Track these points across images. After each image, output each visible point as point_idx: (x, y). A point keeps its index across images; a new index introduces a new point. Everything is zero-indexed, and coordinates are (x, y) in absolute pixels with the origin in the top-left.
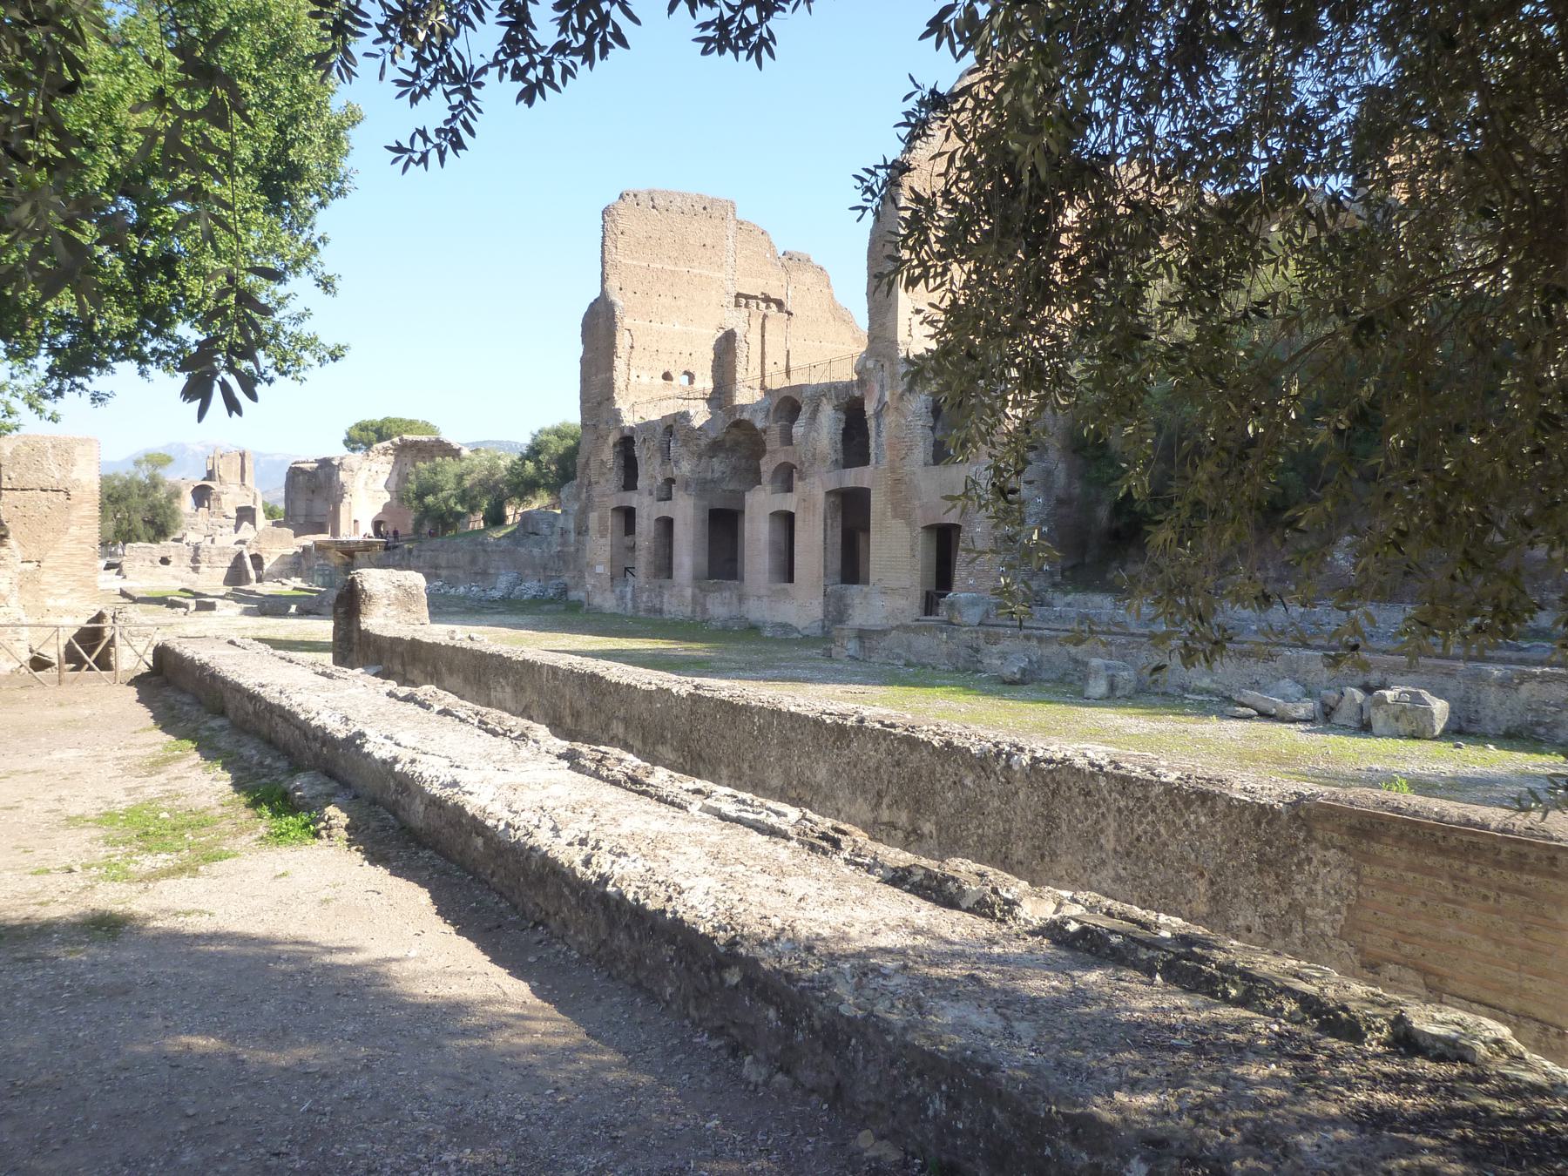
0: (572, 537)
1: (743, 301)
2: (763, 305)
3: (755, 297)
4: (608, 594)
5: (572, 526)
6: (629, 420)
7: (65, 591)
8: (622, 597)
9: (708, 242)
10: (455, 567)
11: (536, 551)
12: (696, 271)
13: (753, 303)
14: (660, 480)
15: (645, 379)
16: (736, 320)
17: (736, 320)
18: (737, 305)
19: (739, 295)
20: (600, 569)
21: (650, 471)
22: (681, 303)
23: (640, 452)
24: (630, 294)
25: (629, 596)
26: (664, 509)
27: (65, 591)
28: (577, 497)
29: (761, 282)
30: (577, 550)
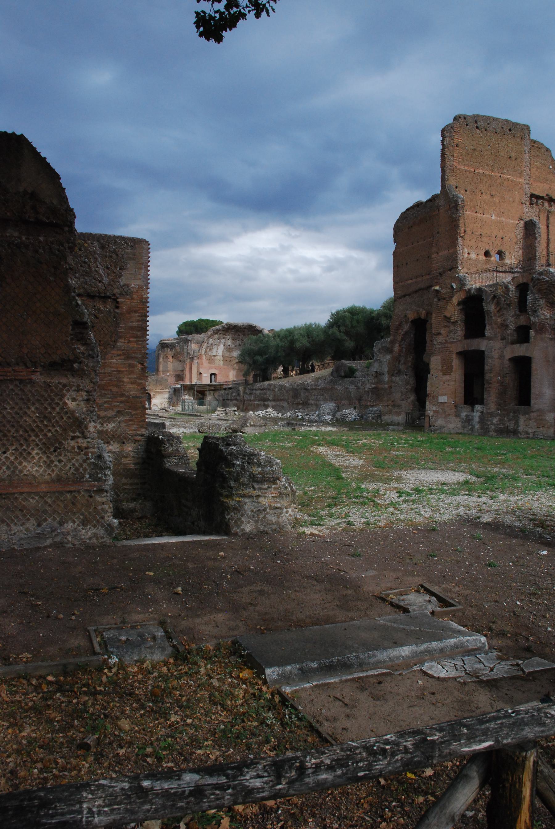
0: (386, 378)
1: (534, 200)
2: (546, 204)
3: (542, 198)
4: (452, 418)
5: (386, 370)
6: (474, 283)
7: (111, 413)
8: (468, 420)
9: (513, 155)
10: (281, 400)
11: (352, 388)
12: (506, 176)
13: (540, 201)
14: (512, 327)
15: (473, 256)
16: (531, 213)
17: (531, 213)
18: (531, 204)
19: (532, 196)
20: (442, 399)
21: (500, 320)
22: (496, 199)
23: (490, 307)
24: (463, 192)
25: (477, 419)
26: (520, 350)
27: (111, 413)
28: (389, 351)
29: (546, 186)
30: (391, 387)
